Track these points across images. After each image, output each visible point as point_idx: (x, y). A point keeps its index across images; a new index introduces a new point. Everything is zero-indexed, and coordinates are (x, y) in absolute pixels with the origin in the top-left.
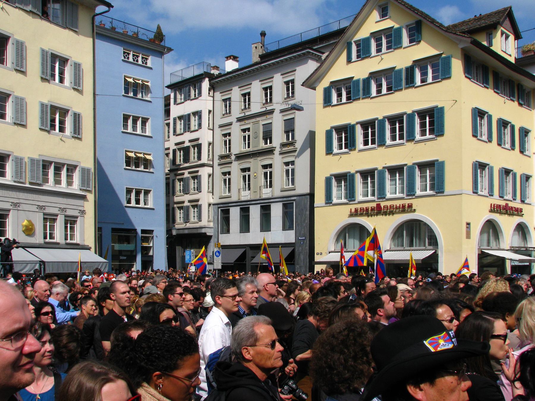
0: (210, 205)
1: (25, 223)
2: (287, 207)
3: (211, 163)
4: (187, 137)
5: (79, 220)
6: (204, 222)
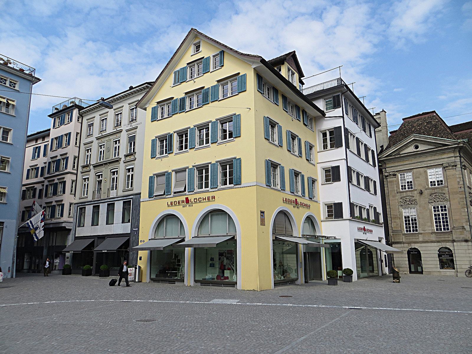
0: (71, 204)
2: (126, 204)
3: (76, 172)
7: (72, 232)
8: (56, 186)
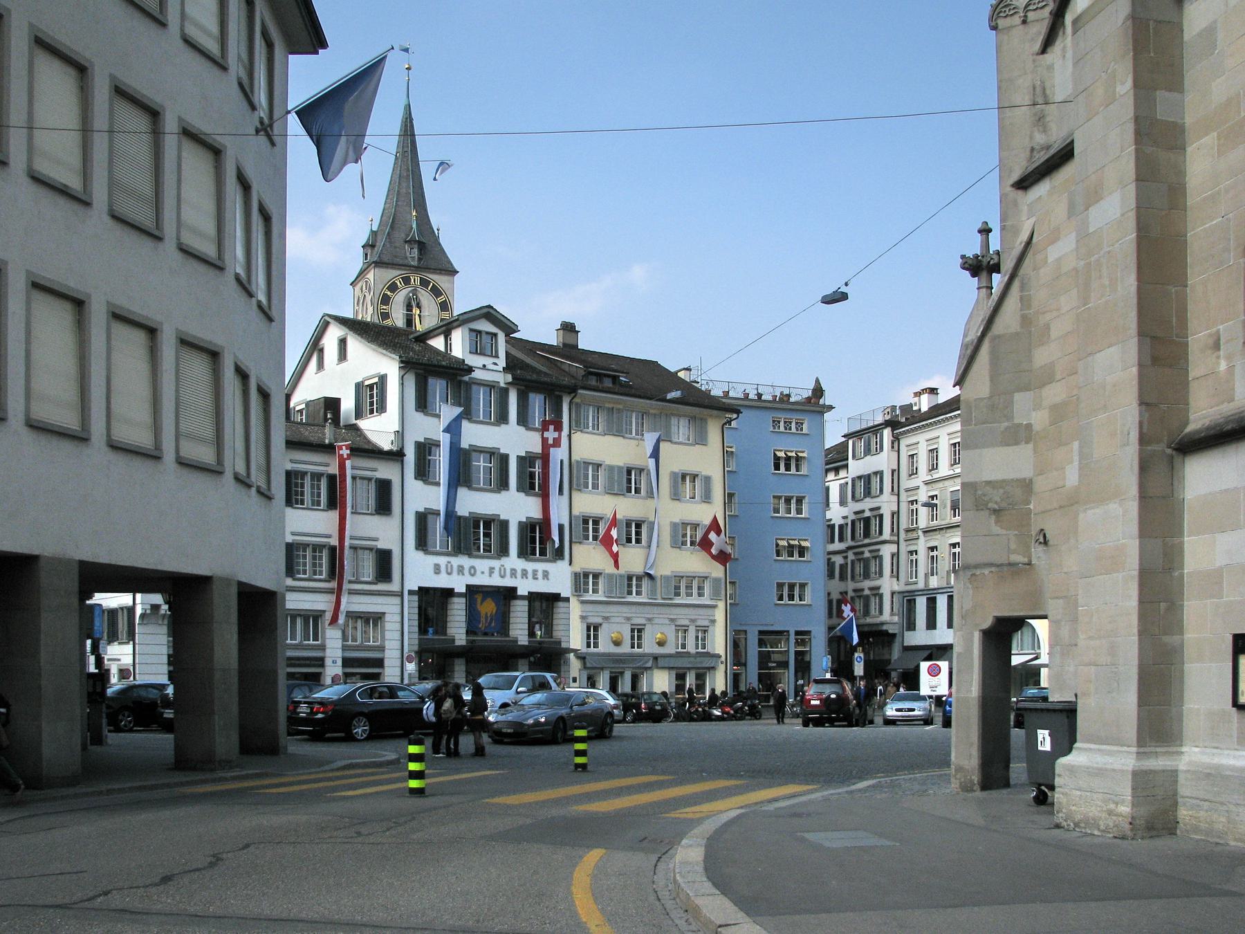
0: (893, 593)
1: (659, 635)
4: (867, 504)
5: (710, 629)
6: (886, 616)
7: (898, 639)
8: (866, 562)
